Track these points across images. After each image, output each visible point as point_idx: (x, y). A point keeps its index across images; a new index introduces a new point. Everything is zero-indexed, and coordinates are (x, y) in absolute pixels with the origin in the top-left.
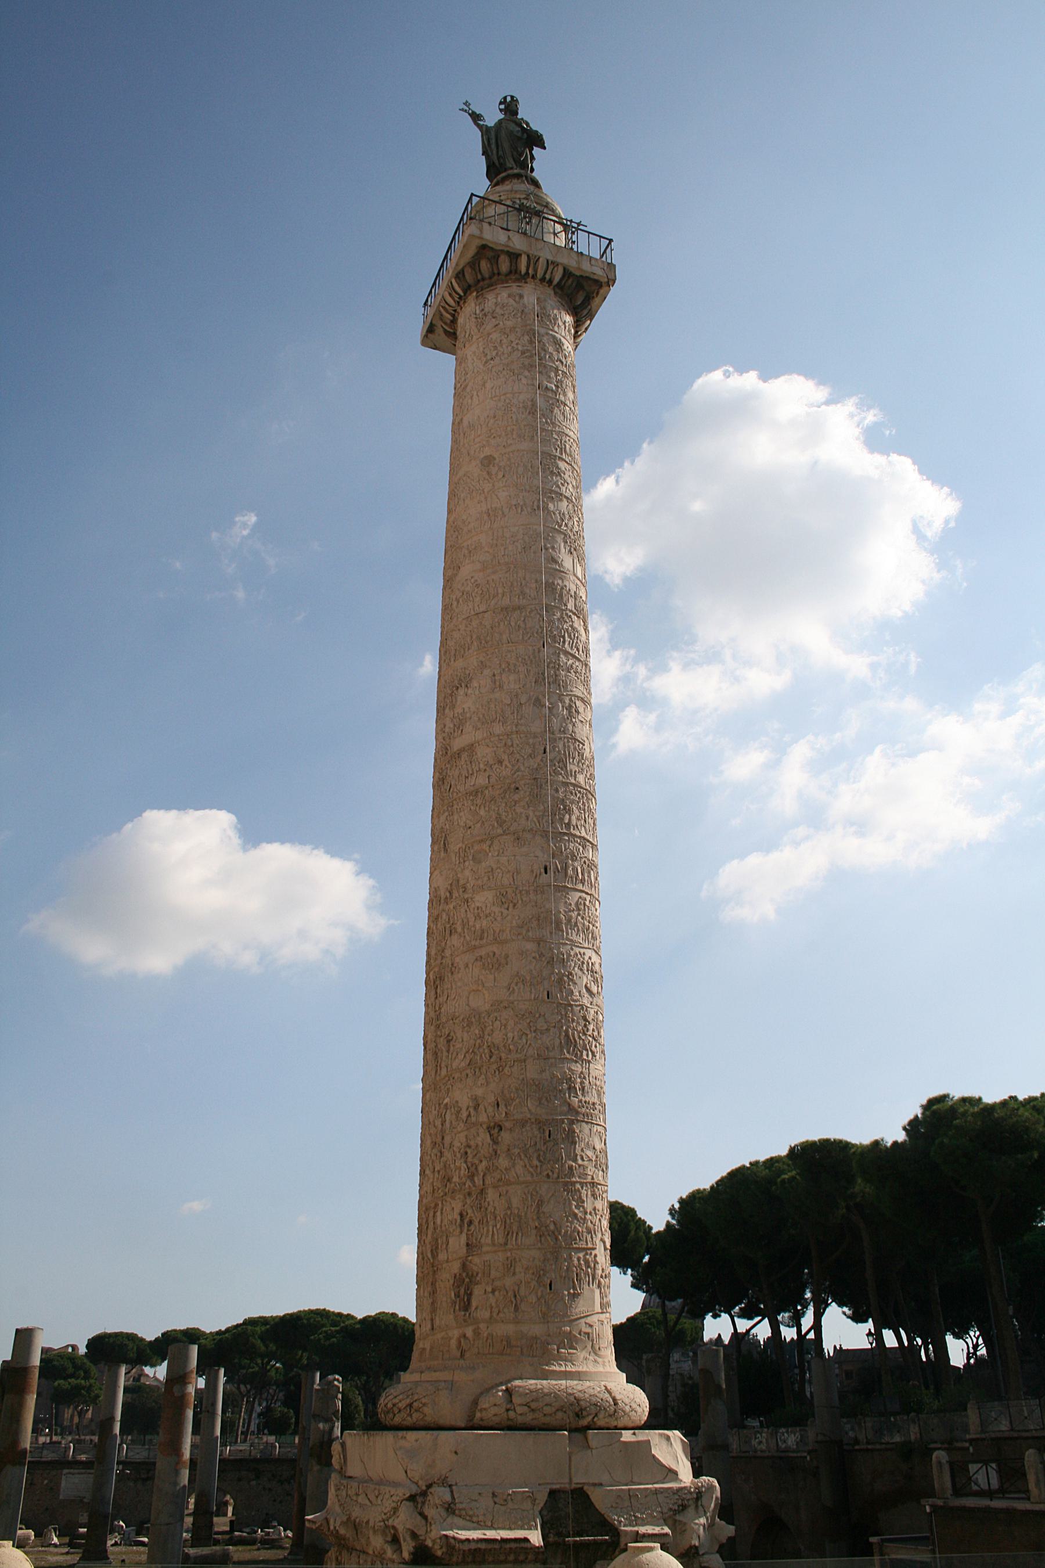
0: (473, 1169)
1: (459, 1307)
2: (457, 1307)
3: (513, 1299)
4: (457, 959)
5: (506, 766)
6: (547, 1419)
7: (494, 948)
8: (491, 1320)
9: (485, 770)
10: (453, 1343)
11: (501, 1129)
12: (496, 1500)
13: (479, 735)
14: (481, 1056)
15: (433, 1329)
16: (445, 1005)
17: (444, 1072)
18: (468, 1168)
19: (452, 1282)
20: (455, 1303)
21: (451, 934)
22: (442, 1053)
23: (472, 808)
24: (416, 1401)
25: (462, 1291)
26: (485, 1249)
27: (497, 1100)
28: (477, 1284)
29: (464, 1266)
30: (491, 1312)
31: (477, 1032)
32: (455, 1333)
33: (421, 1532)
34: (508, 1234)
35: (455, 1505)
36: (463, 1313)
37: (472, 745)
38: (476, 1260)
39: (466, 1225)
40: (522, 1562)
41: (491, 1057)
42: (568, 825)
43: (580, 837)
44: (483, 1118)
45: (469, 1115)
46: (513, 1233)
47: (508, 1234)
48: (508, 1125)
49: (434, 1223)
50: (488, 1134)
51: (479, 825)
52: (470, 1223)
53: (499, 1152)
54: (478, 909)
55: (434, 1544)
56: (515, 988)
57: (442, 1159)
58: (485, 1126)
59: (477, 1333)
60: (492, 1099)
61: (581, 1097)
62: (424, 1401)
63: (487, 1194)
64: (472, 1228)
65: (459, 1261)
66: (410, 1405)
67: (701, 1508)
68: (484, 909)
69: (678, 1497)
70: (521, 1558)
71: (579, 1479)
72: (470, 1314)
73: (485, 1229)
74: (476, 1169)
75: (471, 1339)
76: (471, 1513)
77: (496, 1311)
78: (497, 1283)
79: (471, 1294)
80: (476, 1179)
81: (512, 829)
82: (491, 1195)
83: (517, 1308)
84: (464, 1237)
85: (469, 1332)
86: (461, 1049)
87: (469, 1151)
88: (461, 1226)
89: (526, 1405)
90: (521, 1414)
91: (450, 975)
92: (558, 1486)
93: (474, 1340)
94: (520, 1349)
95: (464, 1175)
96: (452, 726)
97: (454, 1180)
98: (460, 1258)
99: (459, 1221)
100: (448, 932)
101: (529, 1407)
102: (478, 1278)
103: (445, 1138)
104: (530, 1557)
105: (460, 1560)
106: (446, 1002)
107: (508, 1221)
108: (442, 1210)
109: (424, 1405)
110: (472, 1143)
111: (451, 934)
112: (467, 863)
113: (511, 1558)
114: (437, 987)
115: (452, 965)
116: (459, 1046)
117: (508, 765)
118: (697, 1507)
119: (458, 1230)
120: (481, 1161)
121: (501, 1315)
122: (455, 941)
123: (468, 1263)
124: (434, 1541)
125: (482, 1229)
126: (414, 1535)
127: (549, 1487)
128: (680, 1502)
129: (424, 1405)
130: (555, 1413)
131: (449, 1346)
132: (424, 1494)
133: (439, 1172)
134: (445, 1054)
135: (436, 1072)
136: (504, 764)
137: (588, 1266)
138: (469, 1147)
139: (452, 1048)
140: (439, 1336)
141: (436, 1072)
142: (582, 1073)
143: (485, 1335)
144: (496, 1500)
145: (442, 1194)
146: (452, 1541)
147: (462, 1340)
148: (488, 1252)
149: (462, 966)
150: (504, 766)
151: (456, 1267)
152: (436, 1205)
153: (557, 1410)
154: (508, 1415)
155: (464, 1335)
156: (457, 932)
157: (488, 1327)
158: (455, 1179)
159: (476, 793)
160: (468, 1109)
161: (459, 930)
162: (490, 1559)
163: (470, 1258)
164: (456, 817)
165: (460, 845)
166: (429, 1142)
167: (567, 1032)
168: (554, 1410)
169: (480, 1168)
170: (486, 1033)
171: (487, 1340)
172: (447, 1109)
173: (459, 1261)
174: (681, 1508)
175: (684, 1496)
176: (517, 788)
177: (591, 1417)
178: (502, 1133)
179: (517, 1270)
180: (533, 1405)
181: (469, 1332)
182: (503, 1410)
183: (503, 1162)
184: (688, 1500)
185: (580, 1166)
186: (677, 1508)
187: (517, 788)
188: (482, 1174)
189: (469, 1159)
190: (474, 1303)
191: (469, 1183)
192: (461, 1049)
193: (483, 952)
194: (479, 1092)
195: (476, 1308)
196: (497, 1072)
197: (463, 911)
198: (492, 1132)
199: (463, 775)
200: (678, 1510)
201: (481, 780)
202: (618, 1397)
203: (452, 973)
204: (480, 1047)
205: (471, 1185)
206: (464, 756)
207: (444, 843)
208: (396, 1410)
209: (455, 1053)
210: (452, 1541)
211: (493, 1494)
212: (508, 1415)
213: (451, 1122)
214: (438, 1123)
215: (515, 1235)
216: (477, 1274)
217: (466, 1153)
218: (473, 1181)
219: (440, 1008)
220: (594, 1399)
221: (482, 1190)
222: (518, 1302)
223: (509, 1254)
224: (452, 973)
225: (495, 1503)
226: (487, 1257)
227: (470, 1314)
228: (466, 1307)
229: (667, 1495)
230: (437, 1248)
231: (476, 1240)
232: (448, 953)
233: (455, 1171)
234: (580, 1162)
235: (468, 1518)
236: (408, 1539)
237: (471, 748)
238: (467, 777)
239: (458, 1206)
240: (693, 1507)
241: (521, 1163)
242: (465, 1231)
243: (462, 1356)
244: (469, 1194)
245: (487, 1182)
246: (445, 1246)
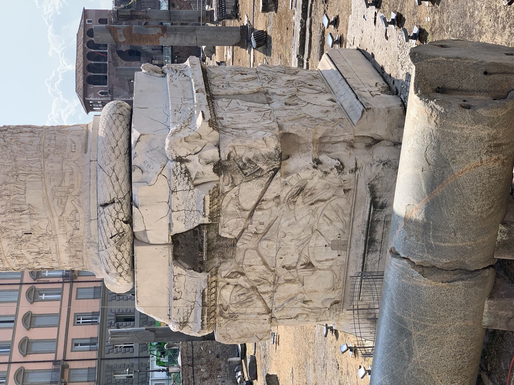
6: (126, 255)
12: (178, 298)
67: (188, 158)
69: (179, 176)
71: (166, 238)
76: (186, 314)
94: (78, 253)
101: (118, 267)
118: (187, 161)
128: (183, 175)
130: (121, 252)
153: (120, 251)
174: (187, 175)
175: (179, 172)
179: (20, 253)
180: (117, 264)
184: (182, 169)
186: (187, 178)
200: (188, 177)
211: (174, 300)
222: (44, 252)
229: (177, 184)
235: (189, 315)
240: (187, 164)
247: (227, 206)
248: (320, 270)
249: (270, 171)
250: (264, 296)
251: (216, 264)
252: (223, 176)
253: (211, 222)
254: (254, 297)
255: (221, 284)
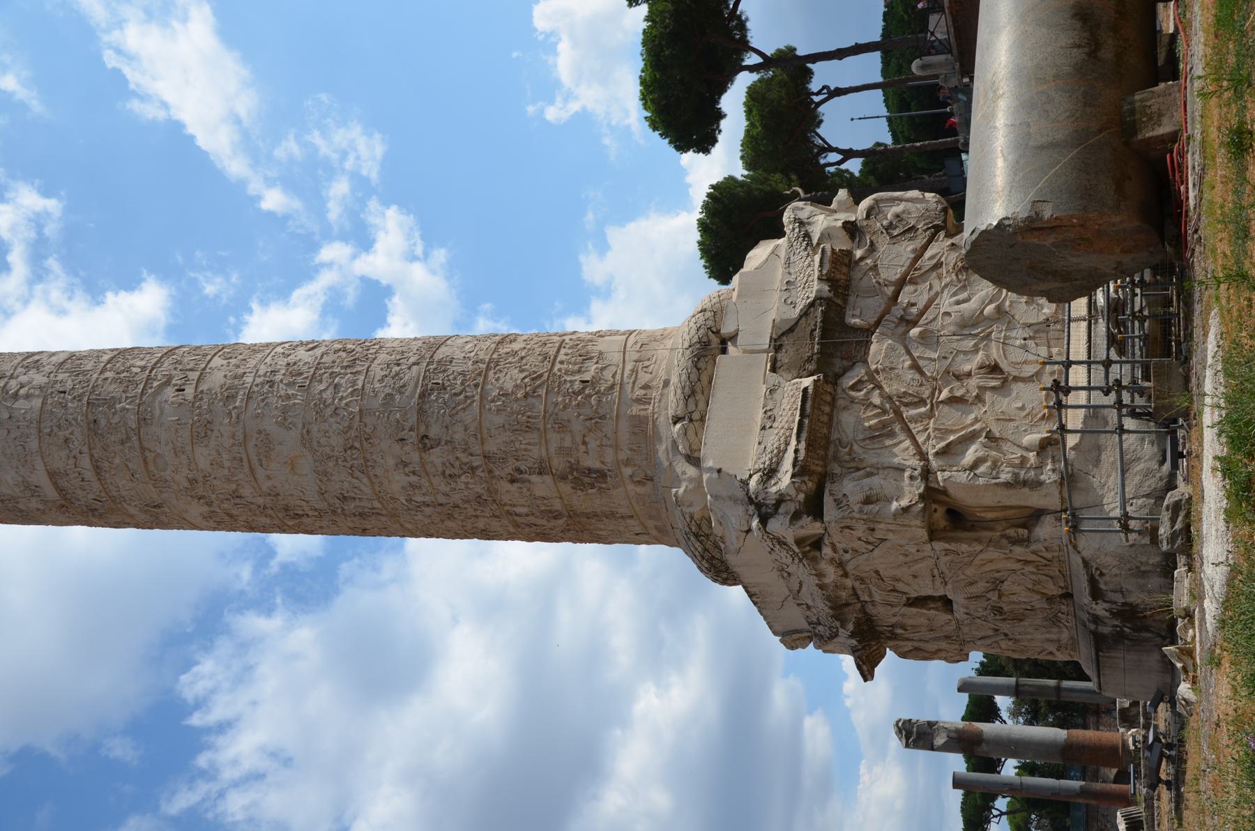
0: (465, 468)
1: (602, 483)
2: (603, 486)
3: (593, 421)
4: (265, 488)
5: (72, 433)
7: (251, 444)
8: (617, 448)
9: (75, 457)
10: (640, 489)
11: (426, 436)
12: (768, 426)
13: (40, 466)
14: (354, 459)
15: (632, 517)
16: (311, 504)
17: (377, 504)
18: (465, 473)
19: (579, 493)
20: (600, 488)
21: (240, 497)
22: (357, 507)
23: (113, 473)
24: (690, 529)
25: (586, 479)
26: (544, 454)
27: (397, 441)
28: (578, 462)
29: (563, 478)
30: (607, 446)
31: (331, 464)
32: (631, 487)
33: (792, 507)
34: (527, 427)
35: (765, 469)
36: (609, 478)
37: (49, 473)
38: (555, 463)
39: (521, 476)
40: (834, 399)
41: (356, 448)
42: (143, 368)
43: (161, 357)
44: (415, 457)
45: (414, 473)
46: (528, 422)
47: (527, 427)
48: (422, 429)
49: (527, 515)
50: (431, 451)
51: (130, 465)
52: (519, 470)
53: (449, 439)
54: (212, 464)
55: (801, 491)
56: (289, 421)
57: (461, 505)
58: (423, 455)
59: (628, 463)
60: (397, 448)
61: (411, 354)
62: (688, 520)
63: (489, 451)
64: (523, 468)
65: (558, 483)
66: (696, 536)
68: (212, 458)
70: (828, 398)
72: (609, 471)
73: (524, 453)
74: (466, 464)
75: (634, 469)
77: (605, 441)
78: (579, 439)
79: (589, 470)
80: (475, 464)
81: (134, 427)
82: (491, 447)
83: (603, 417)
84: (534, 478)
85: (627, 471)
86: (350, 482)
87: (448, 472)
88: (523, 481)
89: (687, 400)
90: (696, 406)
91: (280, 498)
92: (769, 365)
93: (635, 465)
95: (471, 478)
96: (34, 500)
97: (479, 491)
98: (555, 483)
99: (518, 485)
100: (238, 501)
101: (689, 396)
102: (573, 461)
103: (441, 502)
104: (829, 388)
105: (821, 463)
106: (308, 502)
107: (516, 427)
108: (511, 505)
109: (692, 518)
110: (440, 469)
111: (240, 497)
112: (168, 478)
113: (827, 409)
114: (297, 514)
115: (269, 495)
116: (346, 485)
117: (70, 431)
119: (527, 484)
120: (457, 458)
121: (609, 435)
122: (246, 492)
123: (558, 473)
124: (798, 490)
125: (525, 457)
126: (796, 517)
127: (768, 372)
128: (801, 239)
129: (692, 518)
130: (698, 369)
131: (645, 495)
132: (759, 506)
133: (475, 510)
134: (357, 503)
135: (378, 514)
136: (67, 436)
137: (578, 345)
138: (444, 472)
139: (352, 494)
140: (637, 509)
141: (378, 514)
142: (387, 354)
143: (629, 452)
144: (768, 426)
145: (495, 505)
146: (797, 469)
147: (636, 479)
148: (547, 450)
149: (269, 483)
150: (71, 436)
151: (566, 488)
152: (508, 512)
153: (696, 366)
154: (697, 421)
155: (631, 476)
156: (236, 489)
157: (621, 450)
158: (479, 489)
159: (97, 469)
160: (408, 475)
161: (234, 486)
162: (825, 431)
163: (554, 471)
164: (124, 493)
165: (151, 486)
166: (450, 524)
167: (346, 367)
168: (695, 370)
169: (465, 460)
170: (331, 454)
171: (634, 451)
172: (411, 500)
173: (558, 483)
176: (95, 421)
177: (710, 333)
178: (431, 435)
180: (687, 391)
181: (627, 471)
182: (691, 425)
183: (459, 436)
184: (800, 232)
185: (476, 354)
187: (95, 421)
188: (470, 457)
189: (456, 473)
190: (597, 465)
191: (479, 472)
192: (350, 482)
193: (254, 459)
194: (391, 462)
195: (603, 463)
196: (371, 441)
197: (215, 482)
198: (429, 445)
199: (81, 483)
201: (86, 462)
202: (699, 310)
203: (278, 495)
204: (345, 460)
205: (481, 469)
206: (63, 483)
207: (155, 507)
208: (707, 555)
209: (355, 490)
210: (797, 469)
212: (697, 421)
213: (424, 494)
214: (428, 510)
215: (530, 420)
216: (569, 462)
217: (450, 476)
218: (478, 467)
219: (316, 510)
220: (693, 332)
221: (485, 457)
223: (549, 426)
224: (278, 495)
225: (771, 427)
226: (552, 450)
227: (609, 471)
228: (602, 475)
230: (550, 511)
231: (535, 463)
232: (260, 501)
233: (470, 489)
234: (472, 354)
236: (801, 523)
237: (52, 475)
238: (83, 480)
239: (505, 486)
241: (461, 413)
242: (526, 476)
243: (651, 479)
244: (490, 471)
245: (478, 452)
246: (545, 501)
247: (861, 279)
248: (1016, 379)
249: (928, 229)
250: (912, 426)
251: (837, 369)
252: (857, 240)
253: (831, 295)
254: (897, 428)
255: (840, 403)
